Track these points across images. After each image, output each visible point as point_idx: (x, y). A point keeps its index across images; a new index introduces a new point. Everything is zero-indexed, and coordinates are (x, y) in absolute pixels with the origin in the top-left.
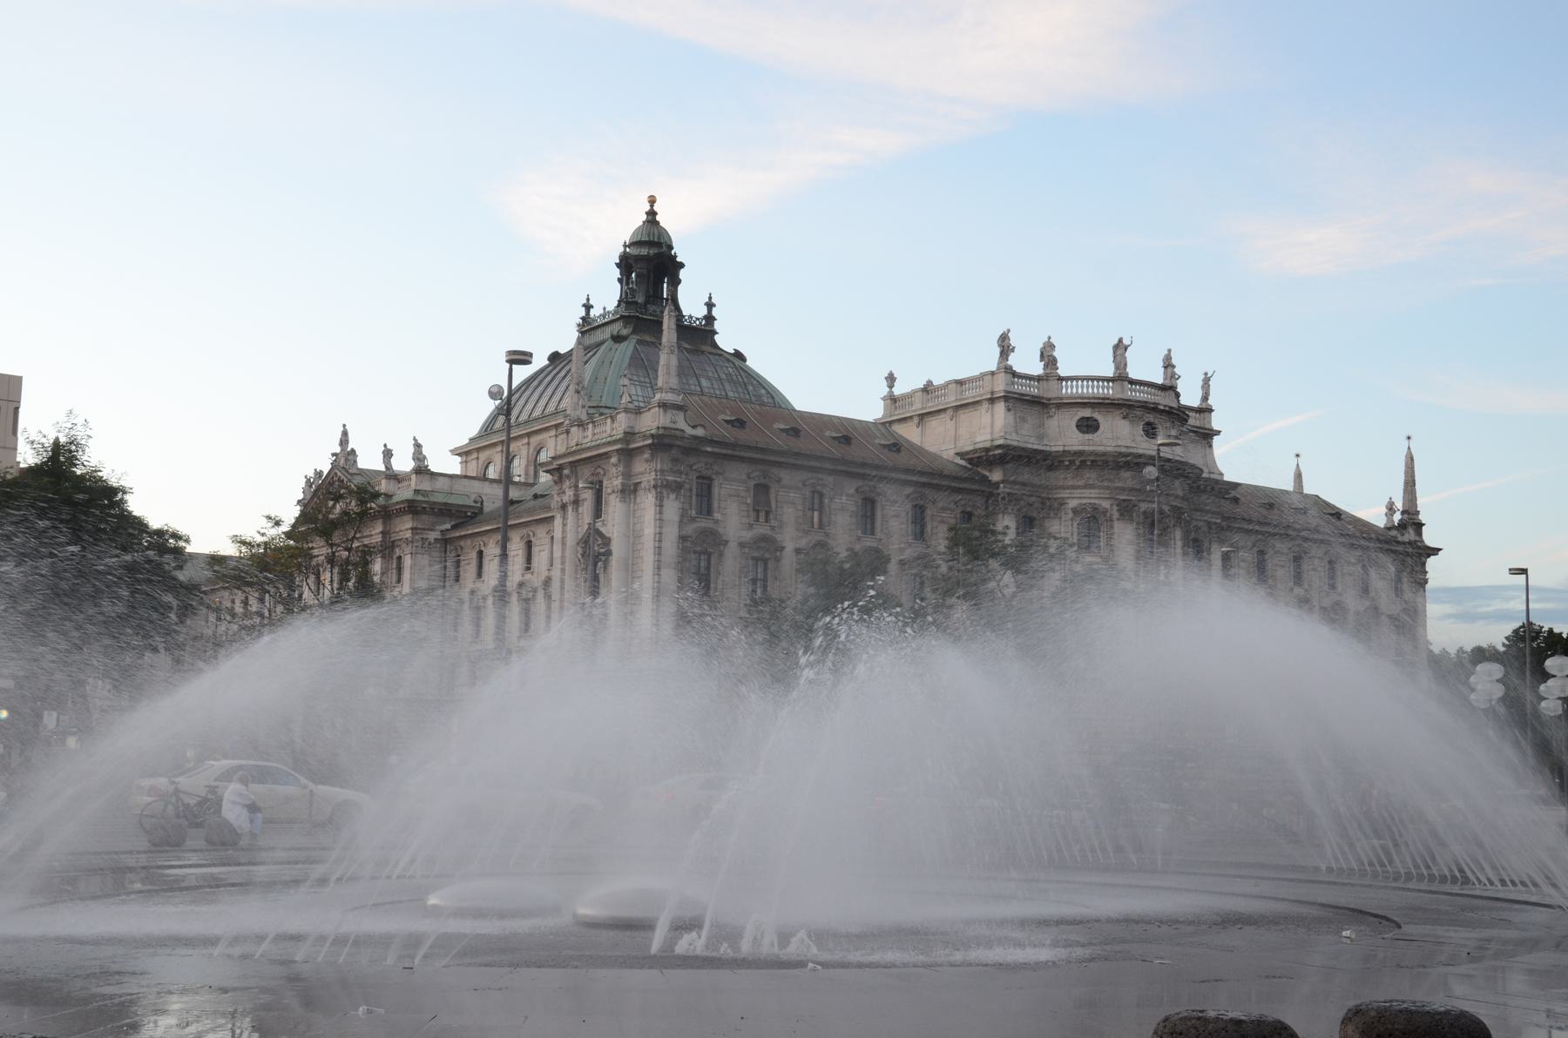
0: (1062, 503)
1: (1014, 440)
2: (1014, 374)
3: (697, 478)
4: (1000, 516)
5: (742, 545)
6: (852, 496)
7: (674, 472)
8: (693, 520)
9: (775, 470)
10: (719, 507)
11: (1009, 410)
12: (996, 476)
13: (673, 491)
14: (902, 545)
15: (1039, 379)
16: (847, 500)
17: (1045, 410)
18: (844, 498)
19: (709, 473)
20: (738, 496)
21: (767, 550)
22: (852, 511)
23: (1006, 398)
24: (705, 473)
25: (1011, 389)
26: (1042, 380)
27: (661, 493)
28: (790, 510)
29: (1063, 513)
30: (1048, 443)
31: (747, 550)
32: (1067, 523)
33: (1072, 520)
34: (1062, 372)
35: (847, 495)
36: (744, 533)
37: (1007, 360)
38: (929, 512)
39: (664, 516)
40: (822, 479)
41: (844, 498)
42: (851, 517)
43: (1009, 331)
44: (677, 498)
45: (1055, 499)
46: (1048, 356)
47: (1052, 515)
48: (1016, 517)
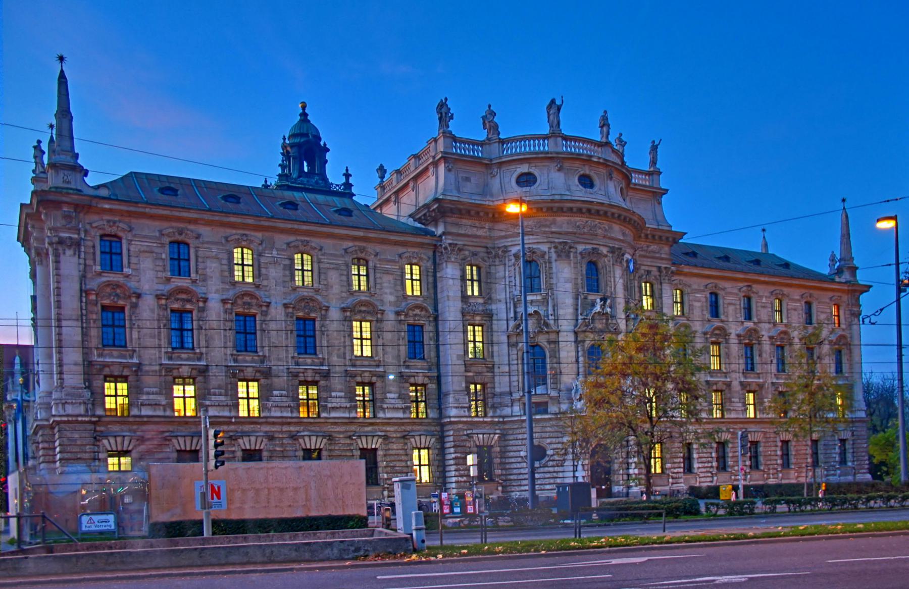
0: (506, 250)
1: (453, 196)
2: (454, 139)
3: (102, 236)
4: (444, 264)
5: (158, 297)
6: (283, 250)
7: (69, 229)
8: (100, 274)
9: (192, 227)
10: (129, 263)
11: (450, 170)
12: (440, 230)
13: (70, 247)
14: (344, 295)
15: (482, 144)
16: (278, 254)
17: (490, 172)
18: (275, 252)
19: (113, 230)
20: (152, 252)
21: (189, 301)
22: (285, 265)
23: (445, 158)
24: (108, 230)
25: (449, 151)
26: (486, 144)
27: (56, 249)
28: (214, 265)
29: (507, 259)
30: (491, 199)
31: (163, 302)
32: (510, 268)
33: (514, 265)
34: (502, 136)
35: (277, 250)
36: (161, 287)
37: (448, 126)
38: (371, 264)
39: (62, 272)
40: (246, 235)
41: (275, 252)
42: (284, 269)
43: (446, 99)
44: (75, 254)
45: (499, 248)
46: (489, 121)
47: (497, 263)
48: (460, 265)
